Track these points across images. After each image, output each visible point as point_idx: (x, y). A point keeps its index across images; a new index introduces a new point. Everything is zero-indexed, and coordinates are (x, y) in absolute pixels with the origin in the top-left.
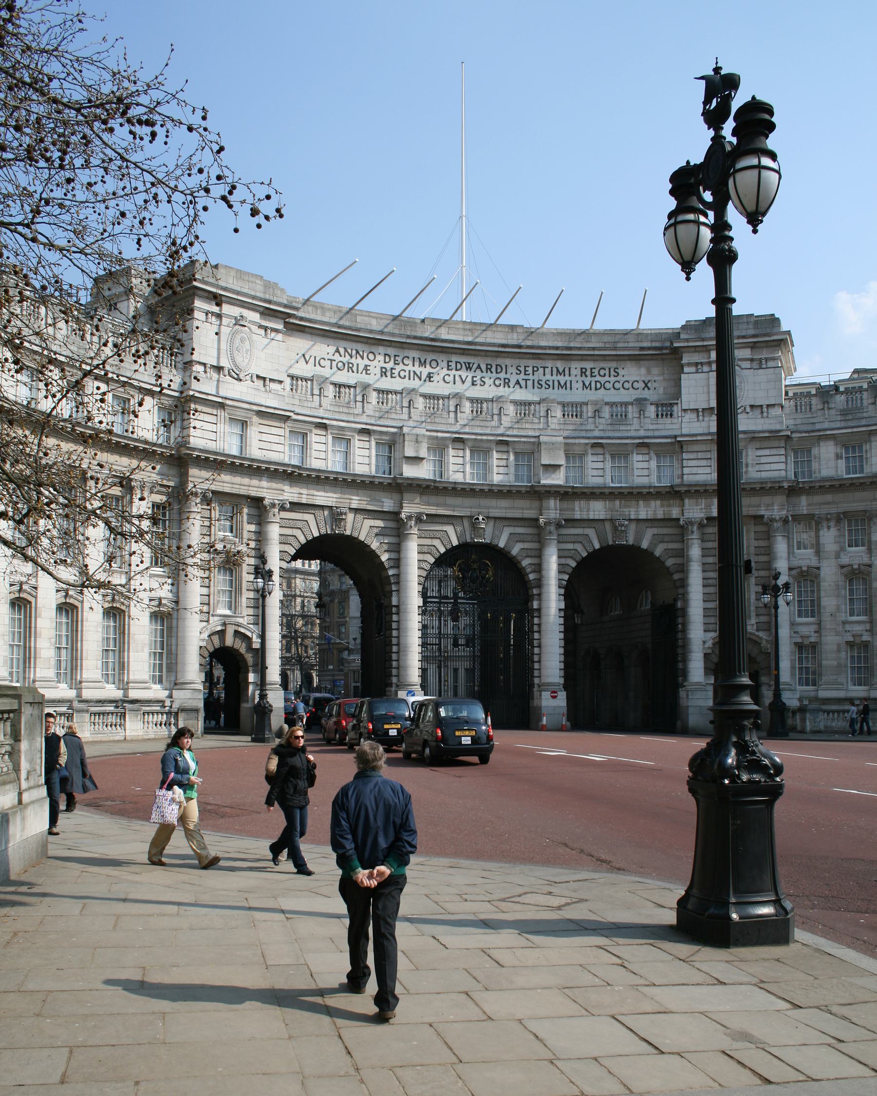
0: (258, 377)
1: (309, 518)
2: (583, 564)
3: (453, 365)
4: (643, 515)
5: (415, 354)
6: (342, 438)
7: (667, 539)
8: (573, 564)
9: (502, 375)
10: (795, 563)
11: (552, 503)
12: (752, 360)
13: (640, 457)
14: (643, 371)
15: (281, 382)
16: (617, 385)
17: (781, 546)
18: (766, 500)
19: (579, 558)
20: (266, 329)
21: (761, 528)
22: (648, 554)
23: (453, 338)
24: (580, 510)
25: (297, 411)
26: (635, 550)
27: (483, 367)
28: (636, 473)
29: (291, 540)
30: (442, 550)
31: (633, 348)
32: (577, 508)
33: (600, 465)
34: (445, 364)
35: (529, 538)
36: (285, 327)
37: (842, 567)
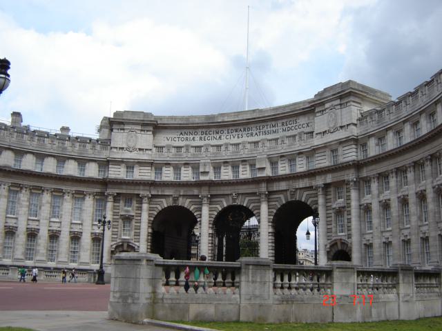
0: (140, 149)
1: (164, 200)
2: (279, 210)
3: (230, 131)
4: (301, 186)
5: (215, 129)
6: (177, 168)
7: (313, 196)
8: (275, 211)
9: (250, 132)
10: (362, 203)
11: (264, 185)
12: (341, 104)
13: (300, 159)
14: (307, 119)
15: (151, 149)
16: (297, 127)
17: (354, 194)
18: (347, 172)
19: (277, 208)
20: (144, 131)
21: (348, 187)
22: (305, 204)
23: (229, 120)
24: (276, 187)
25: (155, 159)
26: (300, 202)
27: (242, 130)
28: (298, 166)
29: (155, 209)
30: (220, 209)
31: (300, 110)
32: (275, 186)
33: (283, 165)
34: (226, 132)
35: (257, 201)
36: (154, 128)
37: (380, 202)
